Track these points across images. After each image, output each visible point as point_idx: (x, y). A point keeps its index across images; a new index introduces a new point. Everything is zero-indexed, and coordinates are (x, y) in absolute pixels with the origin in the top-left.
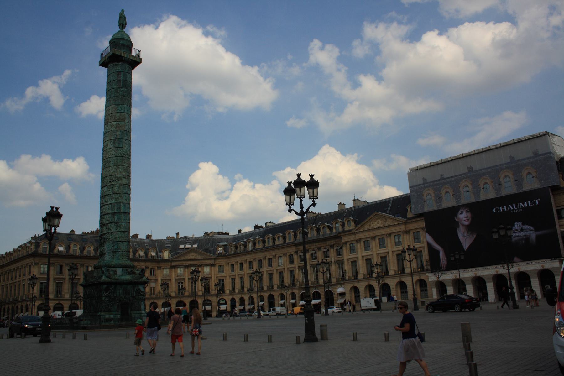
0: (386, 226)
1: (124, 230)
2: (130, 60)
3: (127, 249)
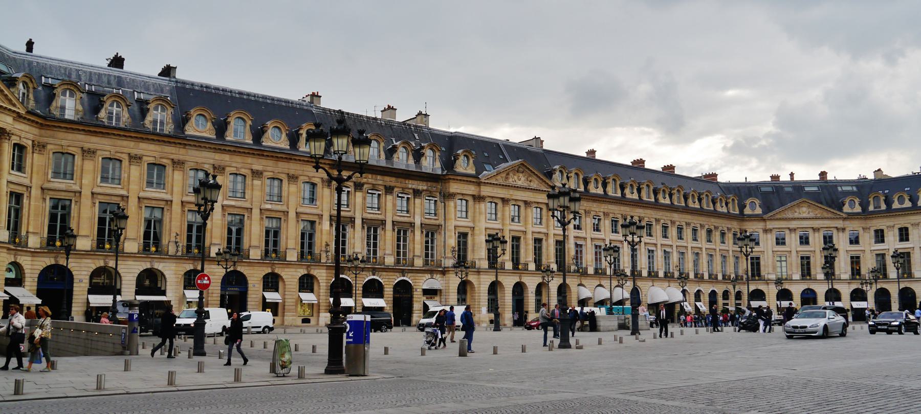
0: (531, 189)
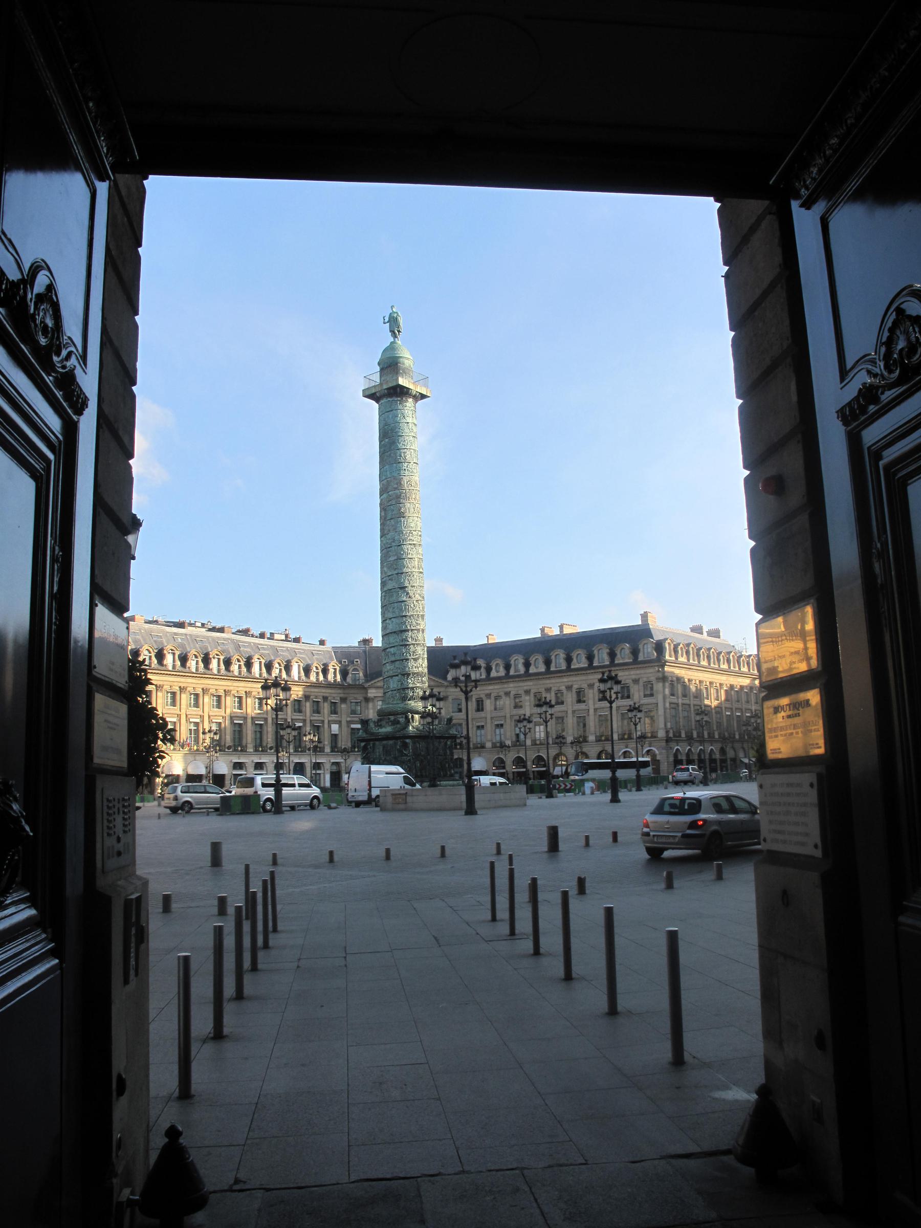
1: (393, 659)
2: (386, 391)
3: (399, 686)
